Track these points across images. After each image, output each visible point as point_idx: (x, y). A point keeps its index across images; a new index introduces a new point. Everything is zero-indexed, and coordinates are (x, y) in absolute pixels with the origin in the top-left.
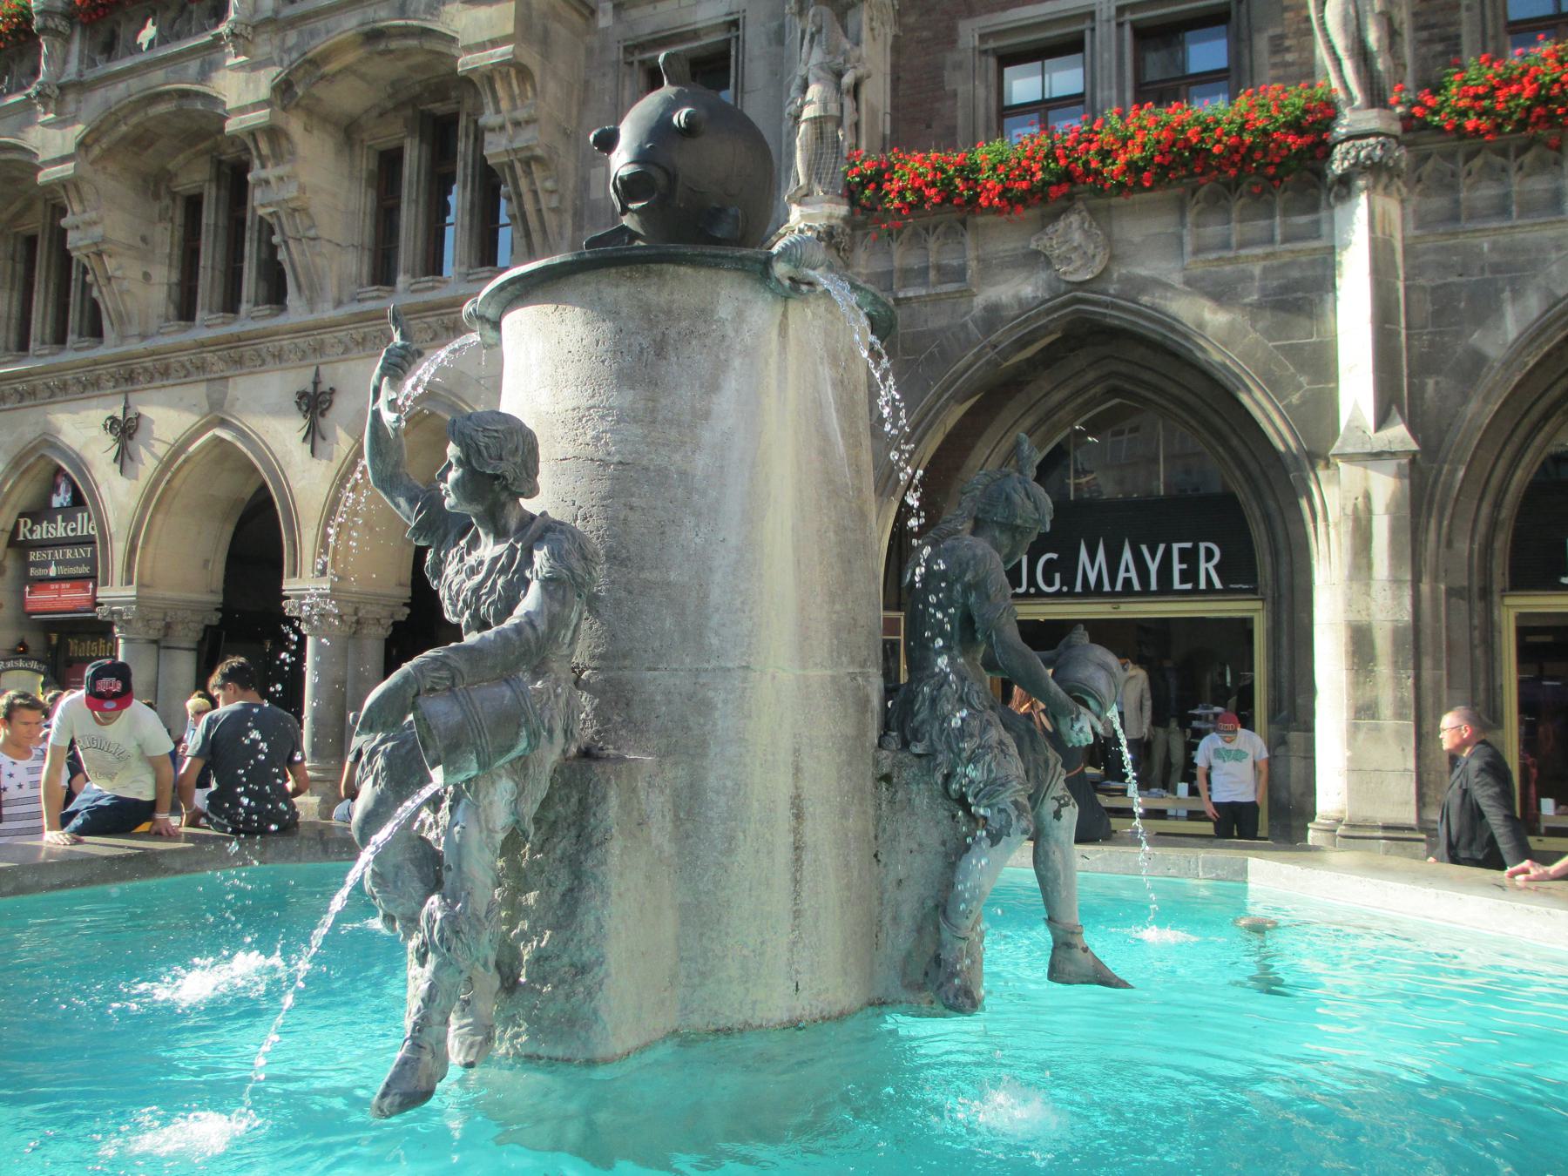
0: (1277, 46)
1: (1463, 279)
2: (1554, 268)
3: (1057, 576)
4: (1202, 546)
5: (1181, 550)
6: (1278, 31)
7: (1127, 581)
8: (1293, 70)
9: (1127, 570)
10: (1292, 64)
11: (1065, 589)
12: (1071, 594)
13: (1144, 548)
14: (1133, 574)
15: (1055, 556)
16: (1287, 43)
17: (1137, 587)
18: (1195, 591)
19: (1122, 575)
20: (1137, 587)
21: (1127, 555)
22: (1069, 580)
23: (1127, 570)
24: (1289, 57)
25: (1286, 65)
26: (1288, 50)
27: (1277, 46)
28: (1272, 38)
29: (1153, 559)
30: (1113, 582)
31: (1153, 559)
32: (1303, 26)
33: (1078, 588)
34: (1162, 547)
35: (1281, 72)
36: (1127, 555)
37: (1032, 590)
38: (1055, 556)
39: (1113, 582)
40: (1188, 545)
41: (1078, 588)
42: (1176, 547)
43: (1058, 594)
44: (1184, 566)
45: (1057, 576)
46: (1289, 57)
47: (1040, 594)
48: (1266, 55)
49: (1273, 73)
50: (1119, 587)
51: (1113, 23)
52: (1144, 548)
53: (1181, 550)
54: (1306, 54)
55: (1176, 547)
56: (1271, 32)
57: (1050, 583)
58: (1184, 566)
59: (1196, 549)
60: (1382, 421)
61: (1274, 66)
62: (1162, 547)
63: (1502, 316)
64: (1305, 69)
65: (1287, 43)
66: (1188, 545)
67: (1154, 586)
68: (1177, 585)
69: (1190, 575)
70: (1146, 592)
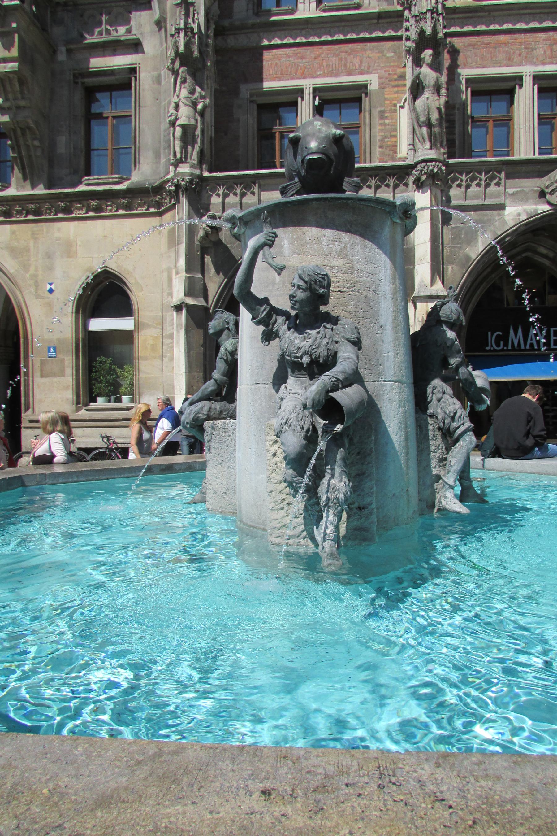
0: (382, 115)
1: (463, 225)
2: (497, 223)
6: (383, 109)
8: (387, 127)
10: (388, 125)
16: (386, 115)
24: (387, 121)
25: (386, 125)
26: (386, 118)
27: (382, 115)
28: (380, 112)
32: (393, 108)
35: (383, 128)
46: (387, 121)
48: (377, 119)
49: (380, 128)
51: (311, 96)
54: (394, 121)
56: (380, 109)
60: (433, 282)
61: (381, 124)
63: (477, 242)
64: (393, 127)
65: (386, 115)
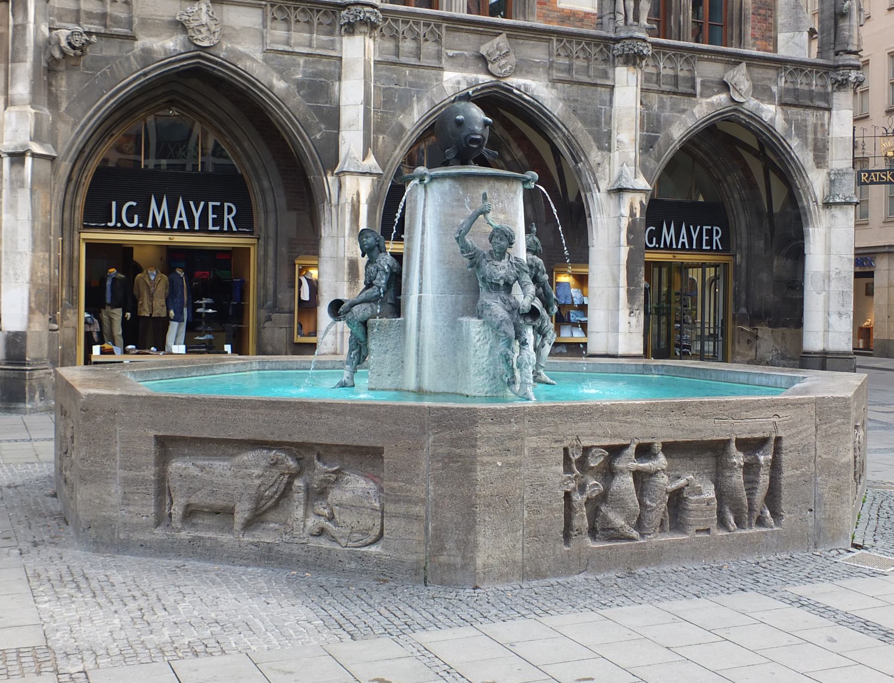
3: (136, 217)
4: (226, 205)
5: (213, 206)
7: (181, 223)
9: (181, 216)
11: (141, 225)
12: (145, 229)
13: (191, 203)
14: (184, 219)
15: (134, 204)
17: (187, 227)
18: (221, 231)
19: (177, 219)
20: (187, 227)
21: (181, 207)
22: (144, 219)
23: (181, 216)
29: (197, 210)
30: (172, 224)
31: (197, 210)
33: (150, 226)
34: (202, 204)
36: (181, 207)
37: (119, 225)
38: (134, 204)
39: (172, 224)
40: (218, 204)
41: (150, 226)
42: (211, 204)
43: (136, 228)
44: (215, 216)
45: (136, 217)
47: (124, 227)
50: (175, 227)
52: (191, 203)
53: (213, 206)
55: (211, 204)
57: (131, 221)
58: (215, 216)
59: (222, 206)
62: (202, 204)
66: (218, 204)
67: (197, 228)
68: (211, 228)
69: (218, 222)
70: (192, 230)
